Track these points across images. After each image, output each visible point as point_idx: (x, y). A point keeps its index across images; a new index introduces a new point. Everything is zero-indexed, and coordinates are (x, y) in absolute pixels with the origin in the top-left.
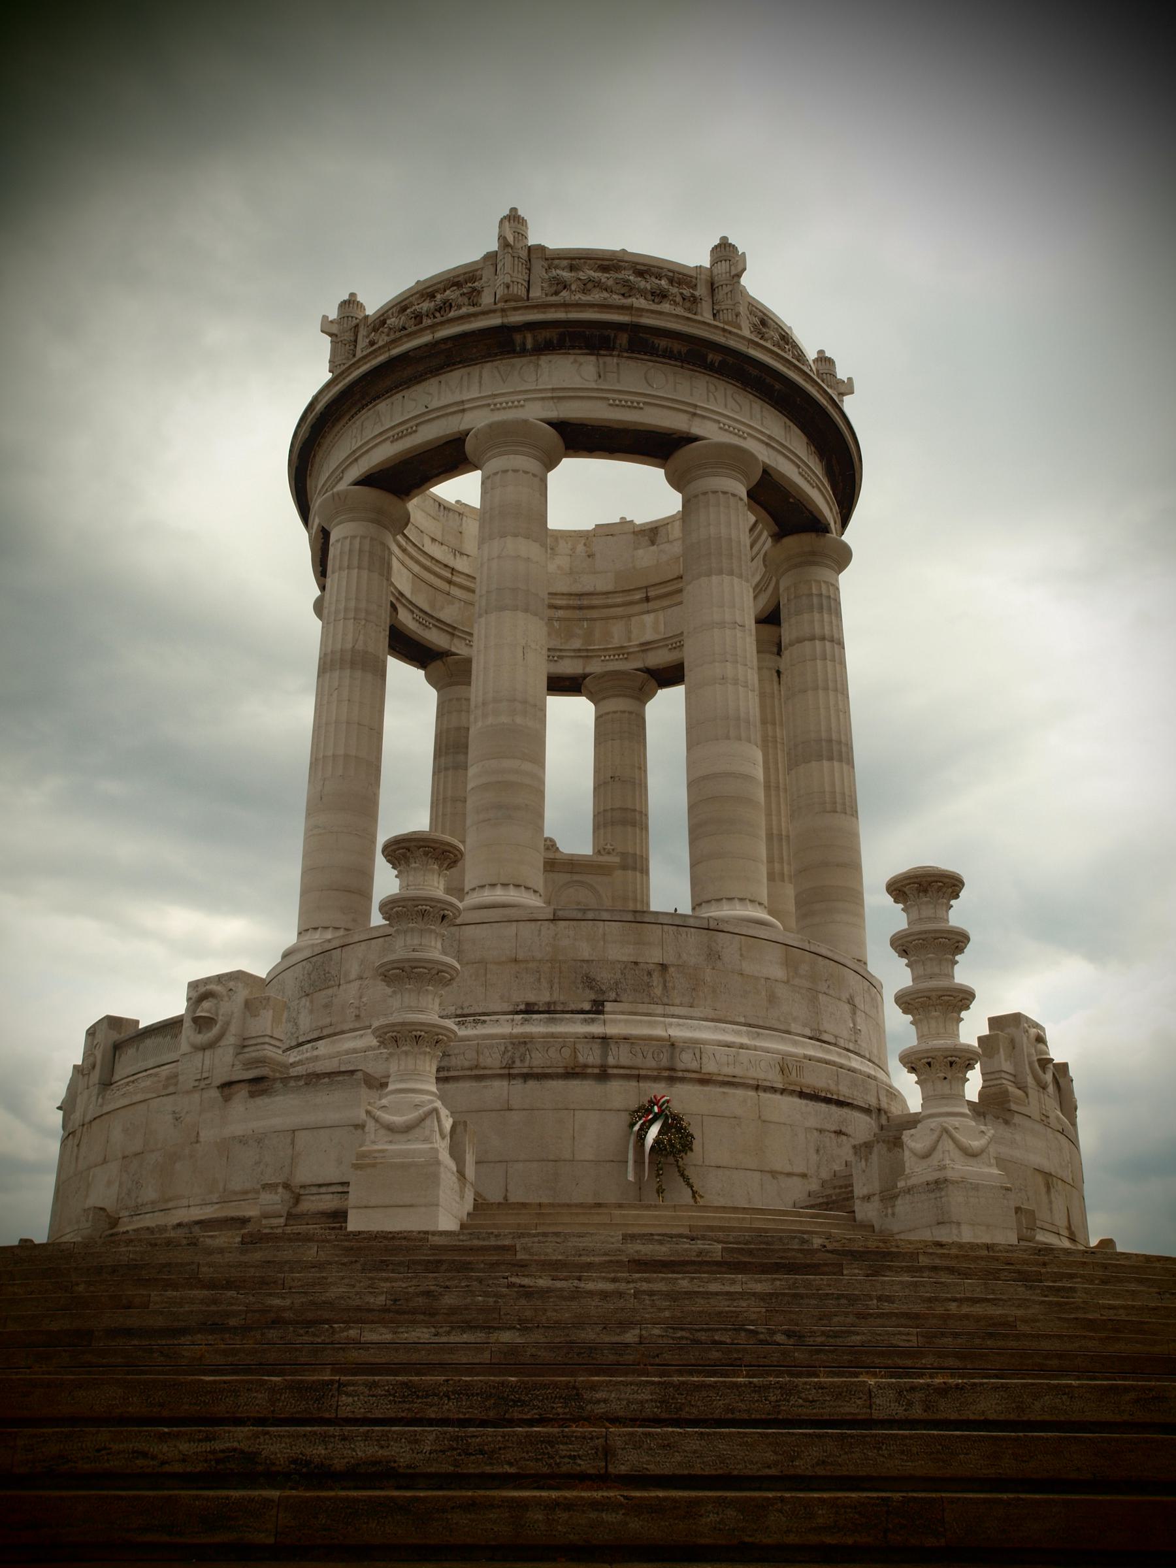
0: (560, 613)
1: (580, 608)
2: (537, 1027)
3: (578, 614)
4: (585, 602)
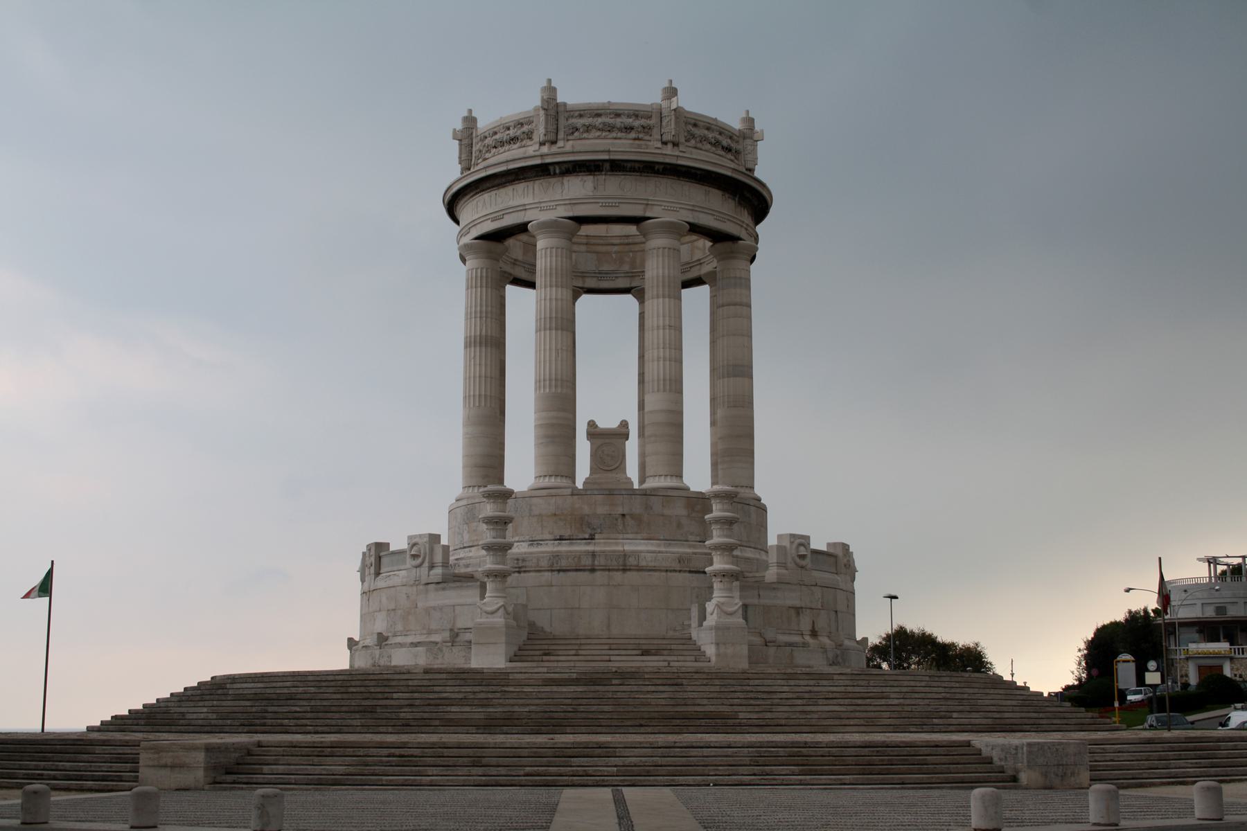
0: (616, 248)
1: (628, 244)
2: (564, 547)
3: (627, 248)
4: (630, 241)
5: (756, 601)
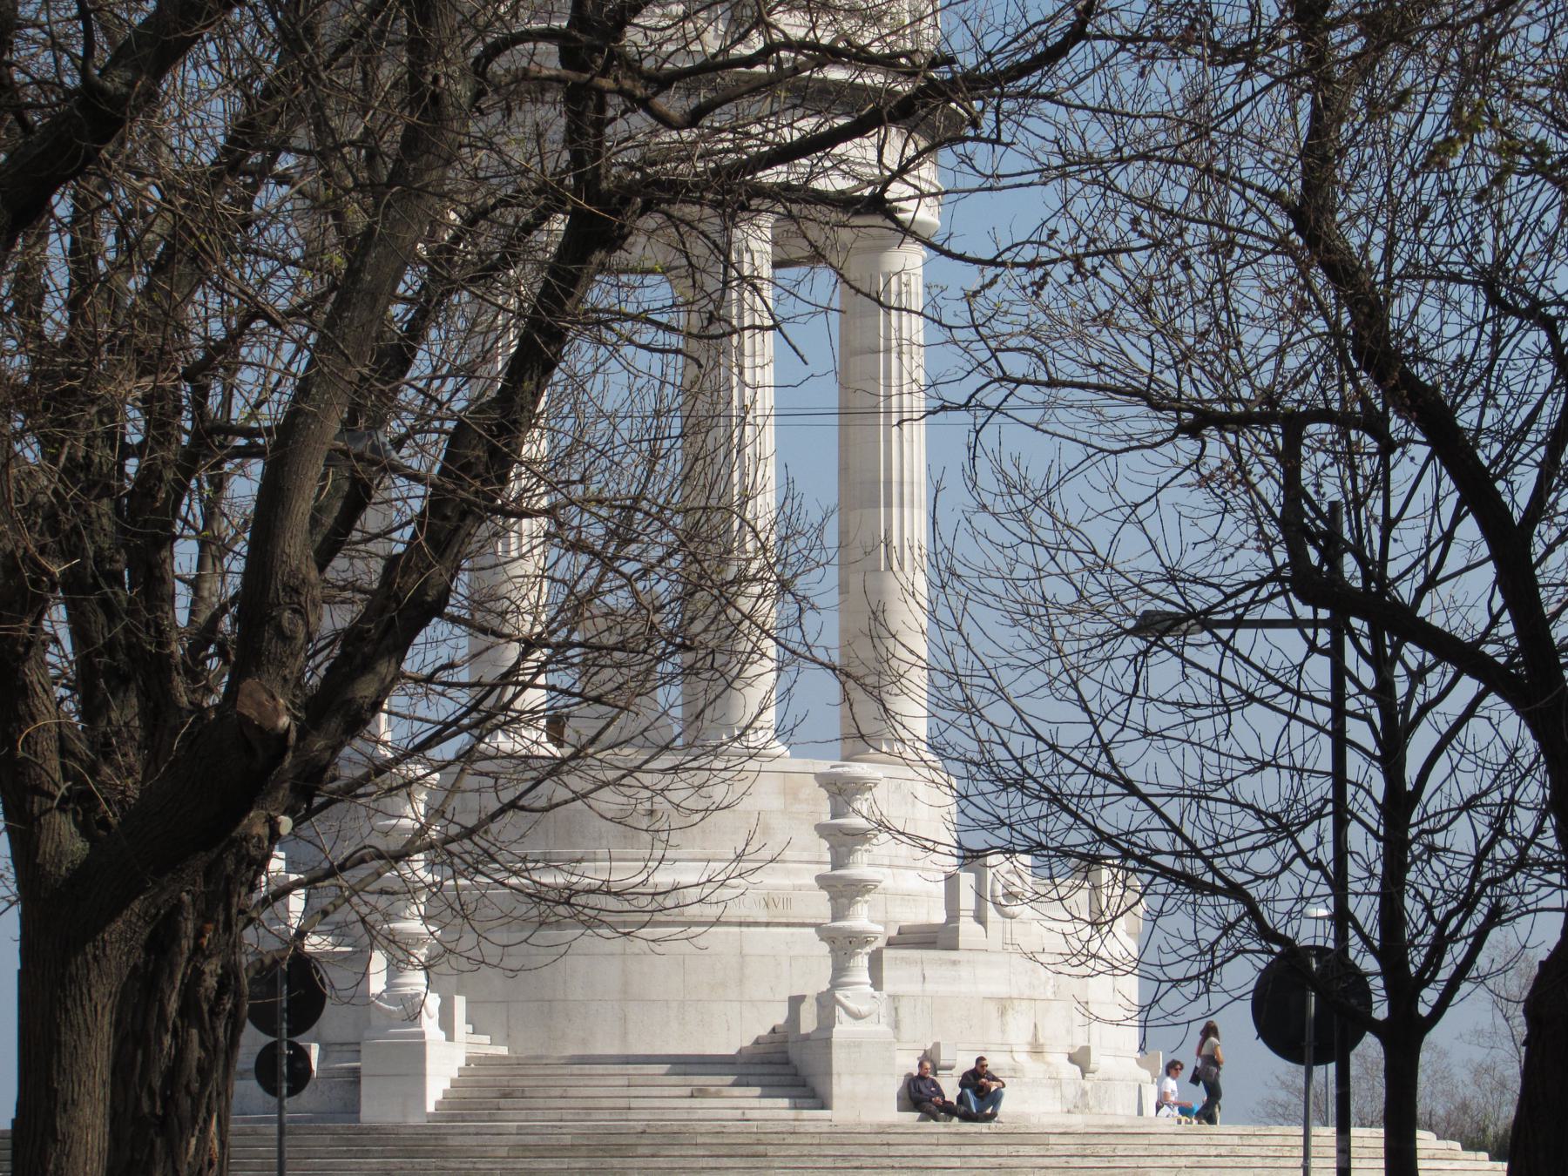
5: (915, 988)
